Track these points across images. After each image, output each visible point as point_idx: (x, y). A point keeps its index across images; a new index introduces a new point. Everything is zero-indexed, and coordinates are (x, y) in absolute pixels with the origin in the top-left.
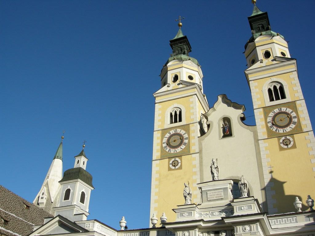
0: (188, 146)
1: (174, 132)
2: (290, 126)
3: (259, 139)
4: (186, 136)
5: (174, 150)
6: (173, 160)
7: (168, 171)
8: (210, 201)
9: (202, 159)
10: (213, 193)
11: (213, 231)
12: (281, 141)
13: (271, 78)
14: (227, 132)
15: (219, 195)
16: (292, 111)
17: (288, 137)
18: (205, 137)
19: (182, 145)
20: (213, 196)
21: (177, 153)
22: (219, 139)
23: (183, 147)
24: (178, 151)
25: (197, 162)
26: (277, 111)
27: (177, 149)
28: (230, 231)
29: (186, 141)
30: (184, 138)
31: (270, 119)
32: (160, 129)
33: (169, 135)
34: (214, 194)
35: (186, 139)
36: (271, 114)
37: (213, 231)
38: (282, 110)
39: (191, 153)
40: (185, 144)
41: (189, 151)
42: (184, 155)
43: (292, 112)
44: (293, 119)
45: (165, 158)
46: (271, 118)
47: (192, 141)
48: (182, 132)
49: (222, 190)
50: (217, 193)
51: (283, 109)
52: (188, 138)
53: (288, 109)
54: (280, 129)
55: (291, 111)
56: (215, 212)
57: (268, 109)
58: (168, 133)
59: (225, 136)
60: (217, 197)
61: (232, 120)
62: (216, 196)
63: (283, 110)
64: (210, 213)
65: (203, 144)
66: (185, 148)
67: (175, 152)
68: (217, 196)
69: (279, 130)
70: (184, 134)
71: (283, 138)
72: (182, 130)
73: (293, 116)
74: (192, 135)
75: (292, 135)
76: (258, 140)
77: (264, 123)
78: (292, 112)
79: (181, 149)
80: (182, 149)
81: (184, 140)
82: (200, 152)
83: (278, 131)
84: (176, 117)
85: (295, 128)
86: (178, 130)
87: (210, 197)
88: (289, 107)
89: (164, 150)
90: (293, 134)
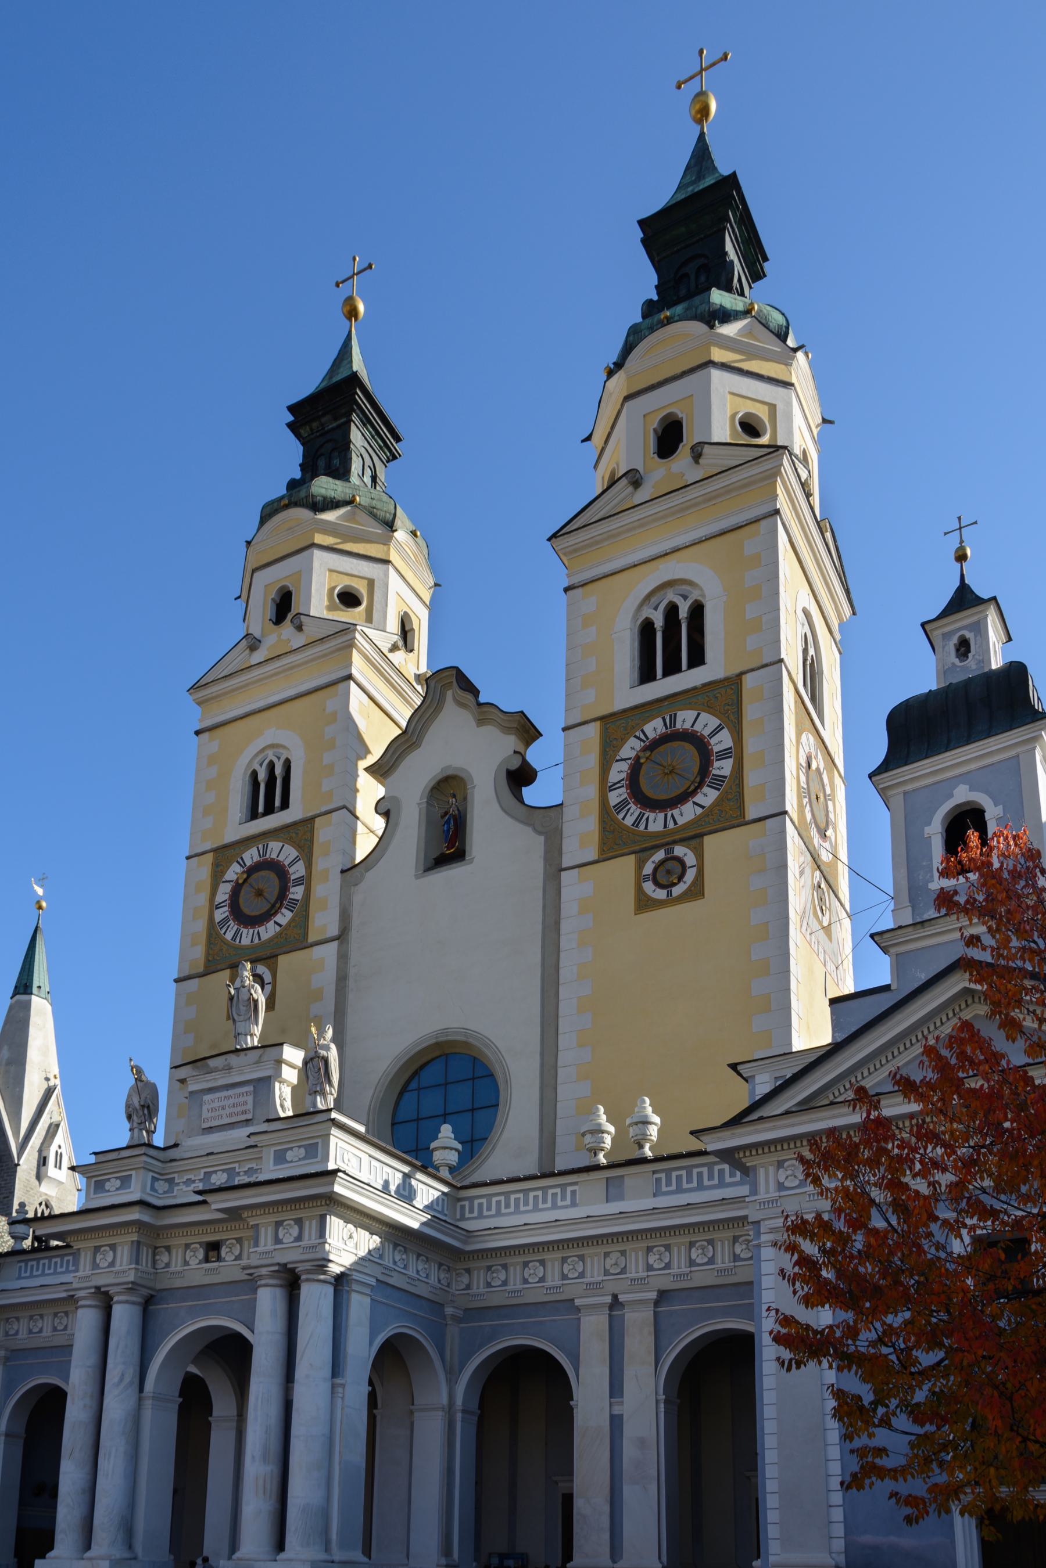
2: (696, 799)
3: (564, 866)
4: (297, 870)
8: (210, 1130)
12: (648, 869)
15: (239, 1109)
16: (718, 722)
17: (679, 851)
18: (367, 870)
22: (417, 877)
23: (284, 917)
26: (654, 728)
29: (297, 893)
30: (293, 877)
31: (619, 771)
35: (299, 881)
38: (678, 726)
40: (292, 905)
44: (716, 764)
47: (319, 890)
49: (250, 1088)
51: (685, 719)
52: (306, 881)
53: (703, 714)
54: (652, 816)
55: (714, 722)
59: (440, 861)
60: (231, 1115)
62: (228, 1111)
63: (684, 721)
65: (357, 899)
68: (233, 1110)
69: (647, 819)
71: (660, 855)
73: (716, 749)
74: (320, 864)
75: (698, 840)
81: (292, 890)
82: (342, 937)
83: (642, 827)
85: (717, 803)
87: (210, 1115)
88: (710, 709)
90: (701, 835)
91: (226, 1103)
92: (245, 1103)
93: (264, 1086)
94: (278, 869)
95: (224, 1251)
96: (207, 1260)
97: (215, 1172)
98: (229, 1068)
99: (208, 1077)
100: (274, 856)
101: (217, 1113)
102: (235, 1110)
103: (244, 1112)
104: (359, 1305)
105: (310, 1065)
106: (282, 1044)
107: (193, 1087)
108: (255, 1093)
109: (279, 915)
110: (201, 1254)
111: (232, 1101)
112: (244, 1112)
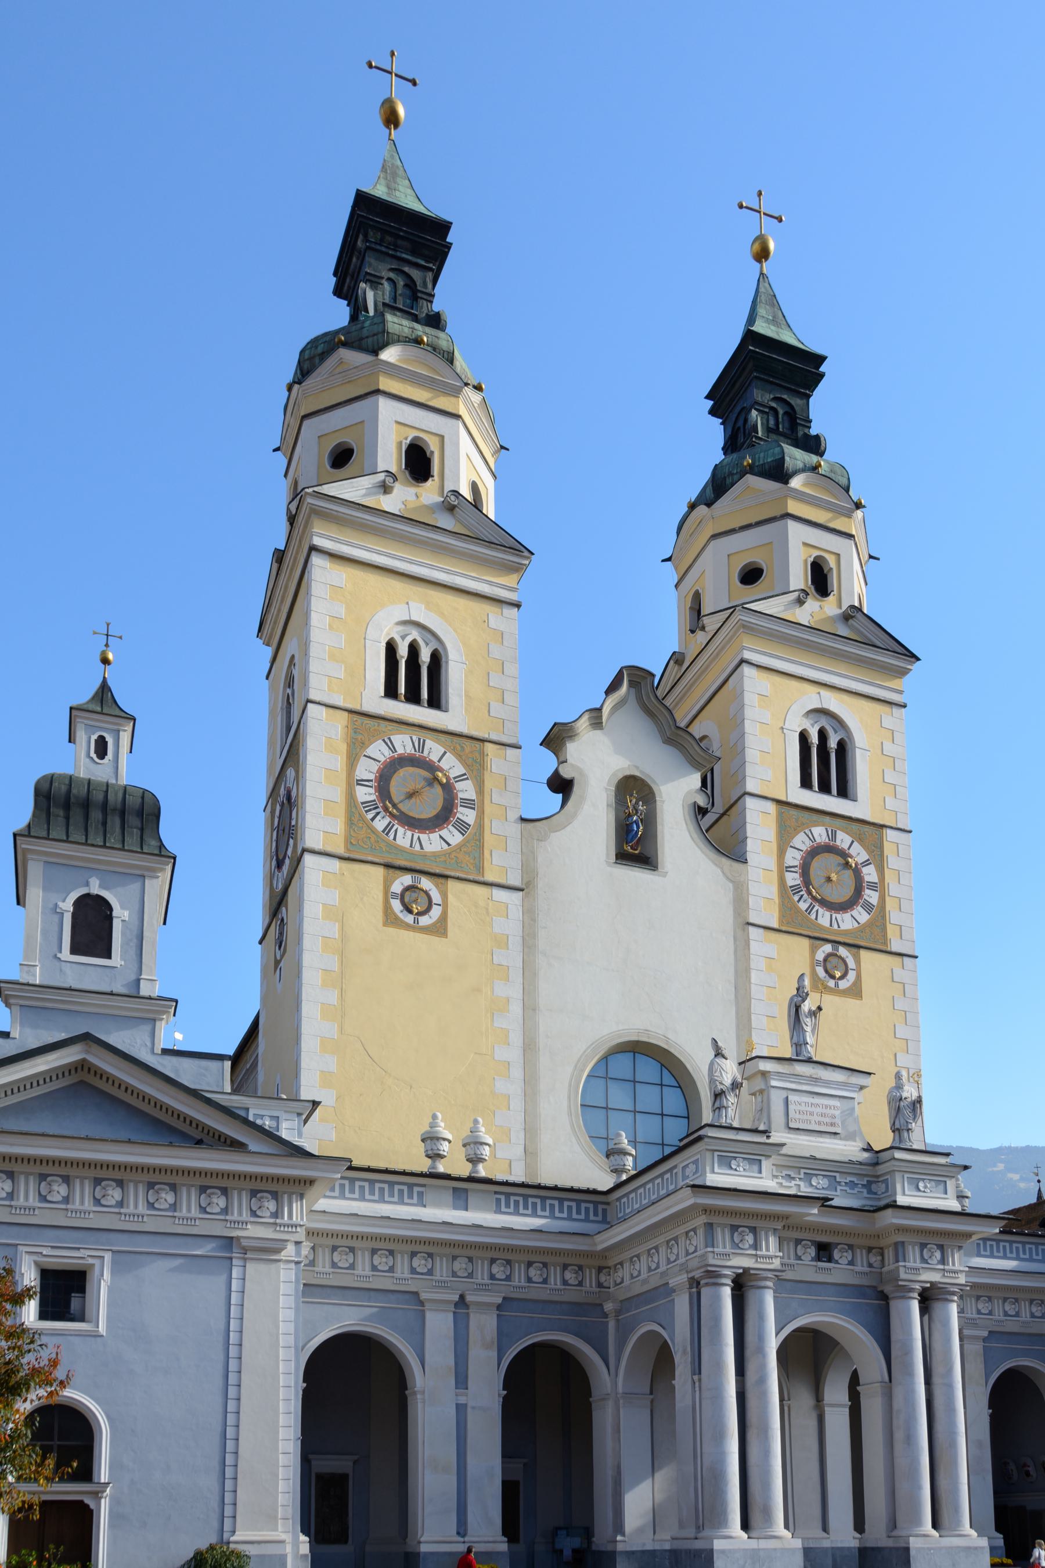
0: (476, 840)
5: (409, 833)
6: (407, 879)
7: (385, 924)
9: (534, 920)
11: (813, 1242)
13: (825, 693)
14: (635, 847)
16: (867, 857)
19: (450, 827)
20: (809, 1117)
21: (425, 856)
24: (428, 848)
25: (511, 925)
26: (820, 834)
27: (423, 837)
28: (864, 1251)
30: (461, 795)
32: (340, 703)
33: (388, 753)
34: (809, 1109)
35: (469, 804)
36: (802, 842)
37: (813, 1242)
38: (838, 843)
39: (489, 877)
40: (462, 827)
41: (480, 869)
42: (458, 874)
43: (866, 863)
45: (370, 858)
46: (798, 855)
48: (452, 766)
50: (819, 1110)
51: (843, 840)
55: (863, 856)
56: (816, 1175)
57: (793, 812)
58: (380, 741)
61: (663, 802)
64: (802, 1176)
66: (460, 846)
67: (417, 847)
70: (460, 778)
72: (448, 754)
73: (867, 878)
76: (749, 924)
77: (772, 864)
78: (866, 863)
79: (445, 846)
80: (449, 845)
81: (460, 809)
84: (415, 675)
86: (429, 743)
88: (861, 841)
89: (362, 818)
91: (813, 1109)
95: (836, 1254)
96: (818, 1258)
97: (816, 1175)
101: (805, 1117)
104: (767, 1303)
110: (812, 1251)
111: (819, 1110)
112: (832, 1125)
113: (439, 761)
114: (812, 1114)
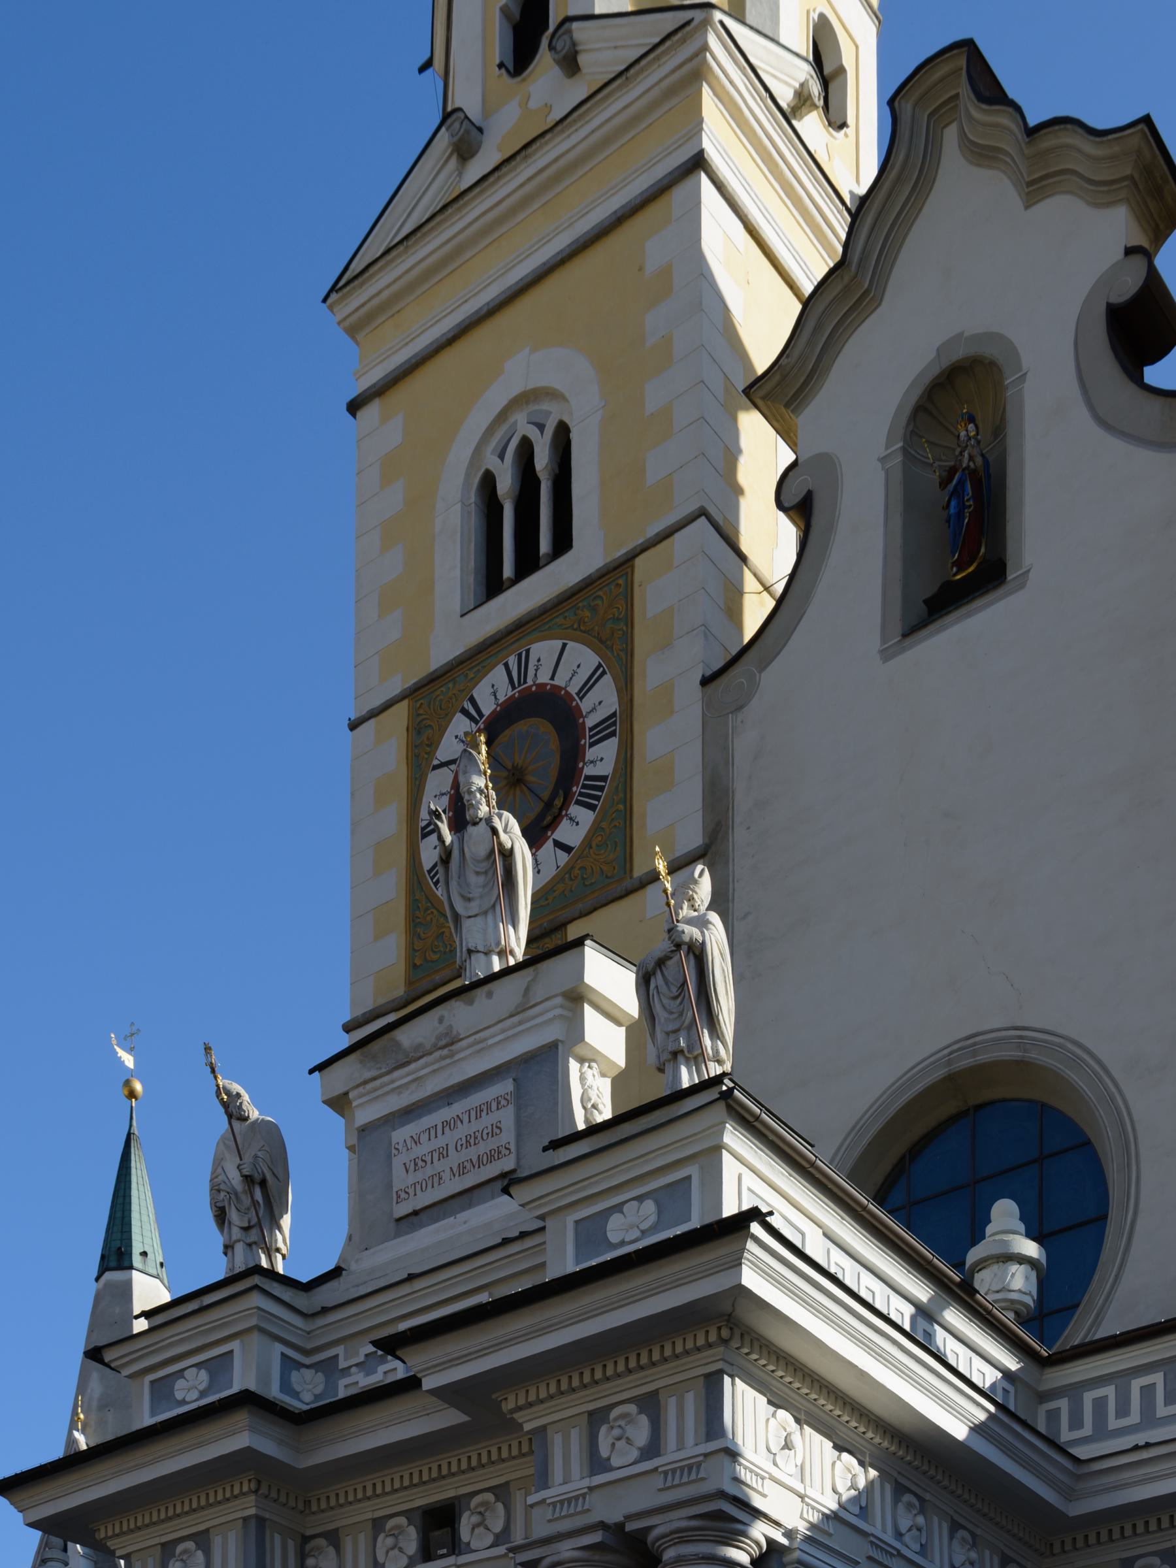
1: (505, 692)
8: (415, 1218)
10: (432, 1131)
15: (483, 1148)
49: (505, 1087)
50: (462, 1131)
60: (462, 1170)
62: (454, 1159)
87: (411, 1179)
92: (497, 1129)
93: (542, 1069)
94: (550, 707)
98: (449, 1041)
99: (401, 1077)
100: (543, 678)
101: (429, 1171)
102: (472, 1153)
103: (494, 1155)
105: (657, 981)
106: (579, 943)
107: (364, 1116)
108: (519, 1098)
109: (565, 823)
111: (462, 1131)
112: (494, 1155)
113: (552, 678)
114: (443, 1154)
